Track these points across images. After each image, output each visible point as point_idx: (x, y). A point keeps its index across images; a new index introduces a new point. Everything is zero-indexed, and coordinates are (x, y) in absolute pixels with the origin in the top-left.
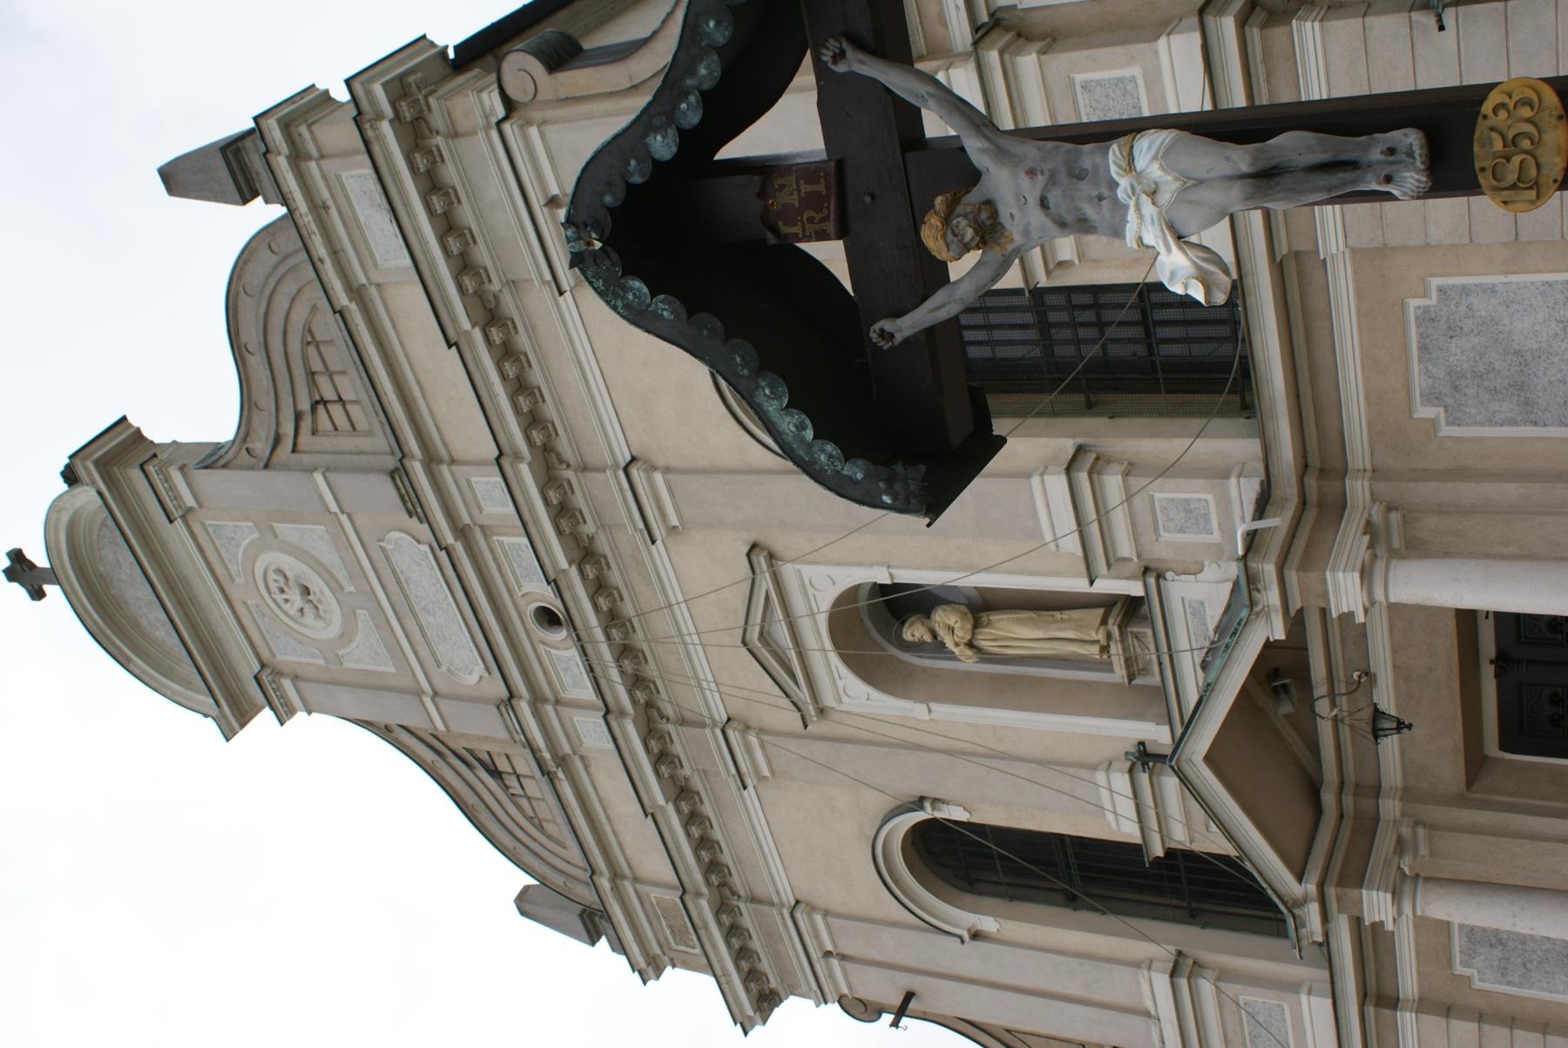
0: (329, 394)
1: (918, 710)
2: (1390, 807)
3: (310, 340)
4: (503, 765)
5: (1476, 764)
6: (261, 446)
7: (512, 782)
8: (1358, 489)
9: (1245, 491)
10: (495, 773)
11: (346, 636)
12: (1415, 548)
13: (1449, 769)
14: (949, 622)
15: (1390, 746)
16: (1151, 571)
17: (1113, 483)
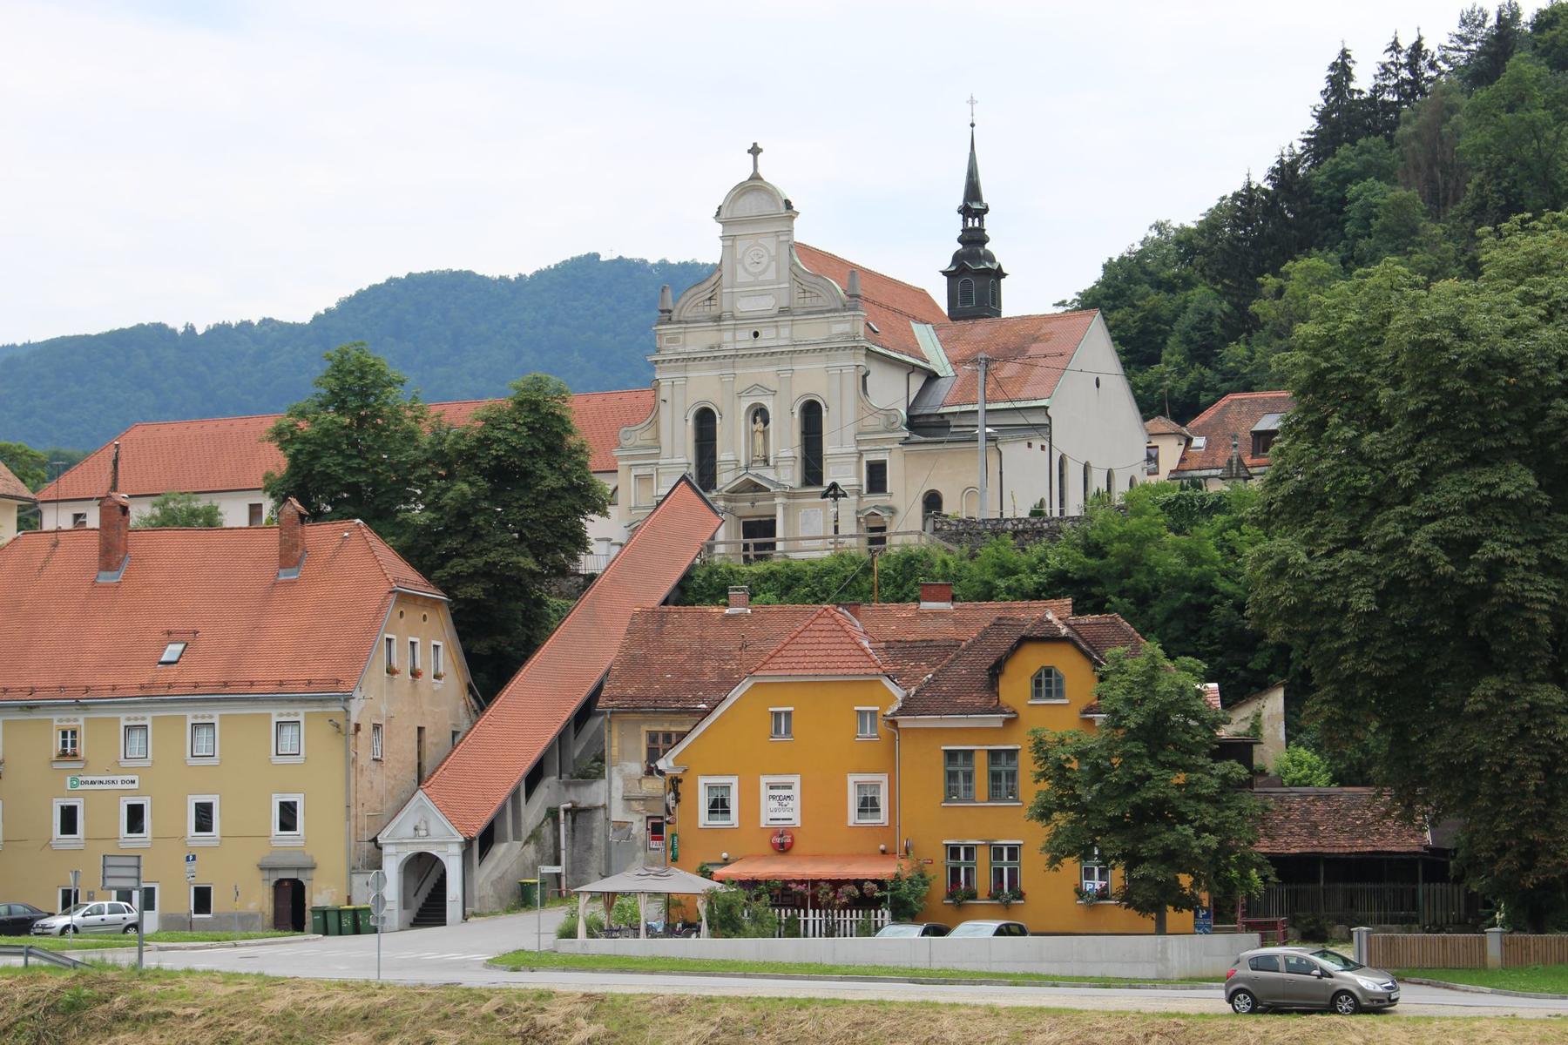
0: (807, 295)
1: (742, 418)
2: (733, 504)
3: (818, 296)
4: (713, 302)
5: (740, 518)
6: (794, 268)
7: (708, 303)
8: (791, 501)
9: (791, 484)
10: (710, 299)
11: (746, 270)
12: (784, 509)
13: (740, 513)
14: (760, 426)
15: (748, 504)
16: (775, 467)
17: (792, 463)
